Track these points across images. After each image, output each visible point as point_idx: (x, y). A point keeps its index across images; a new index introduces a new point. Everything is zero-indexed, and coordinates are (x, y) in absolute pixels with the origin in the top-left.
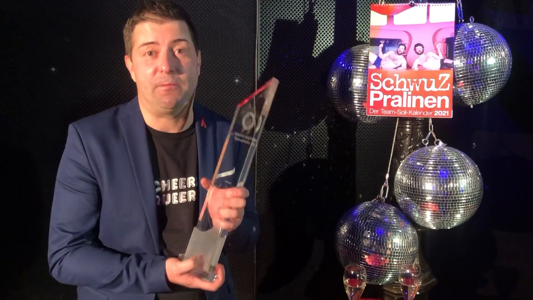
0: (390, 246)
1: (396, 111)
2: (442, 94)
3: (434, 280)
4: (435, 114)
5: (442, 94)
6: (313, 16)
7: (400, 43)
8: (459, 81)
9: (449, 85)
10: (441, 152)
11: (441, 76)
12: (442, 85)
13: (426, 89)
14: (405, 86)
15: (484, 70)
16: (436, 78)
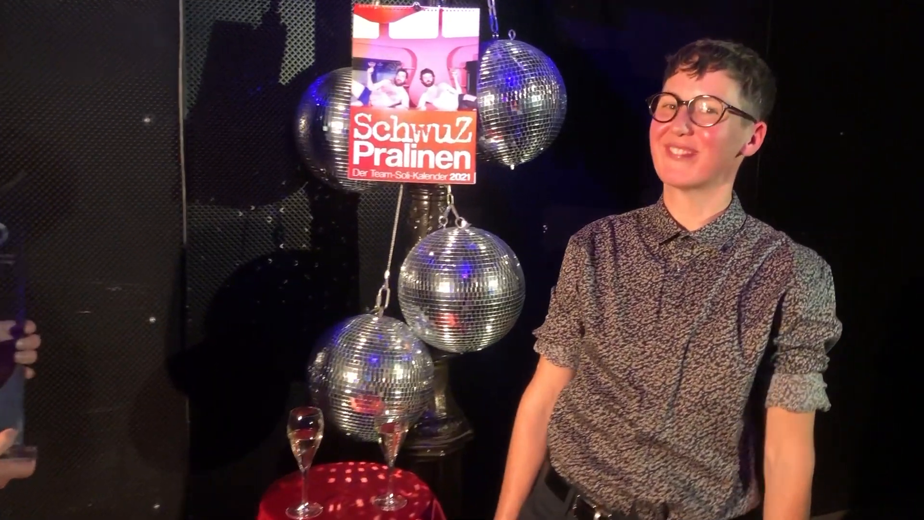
0: (384, 380)
3: (469, 432)
4: (451, 179)
6: (278, 17)
7: (399, 67)
9: (470, 134)
10: (463, 234)
11: (459, 120)
12: (460, 134)
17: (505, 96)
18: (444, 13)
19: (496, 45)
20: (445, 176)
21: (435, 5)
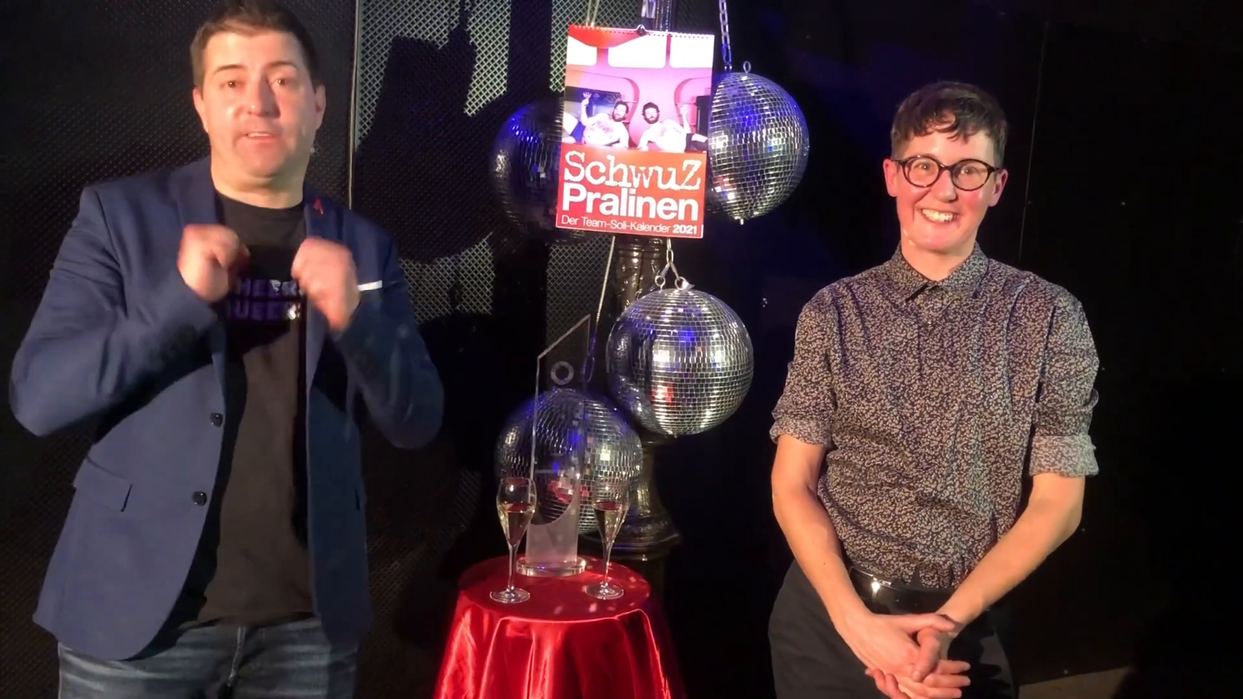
6: (467, 36)
9: (699, 180)
10: (684, 296)
11: (686, 163)
13: (660, 185)
14: (625, 177)
15: (757, 157)
16: (678, 166)
17: (741, 137)
19: (730, 79)
20: (667, 228)
21: (664, 30)
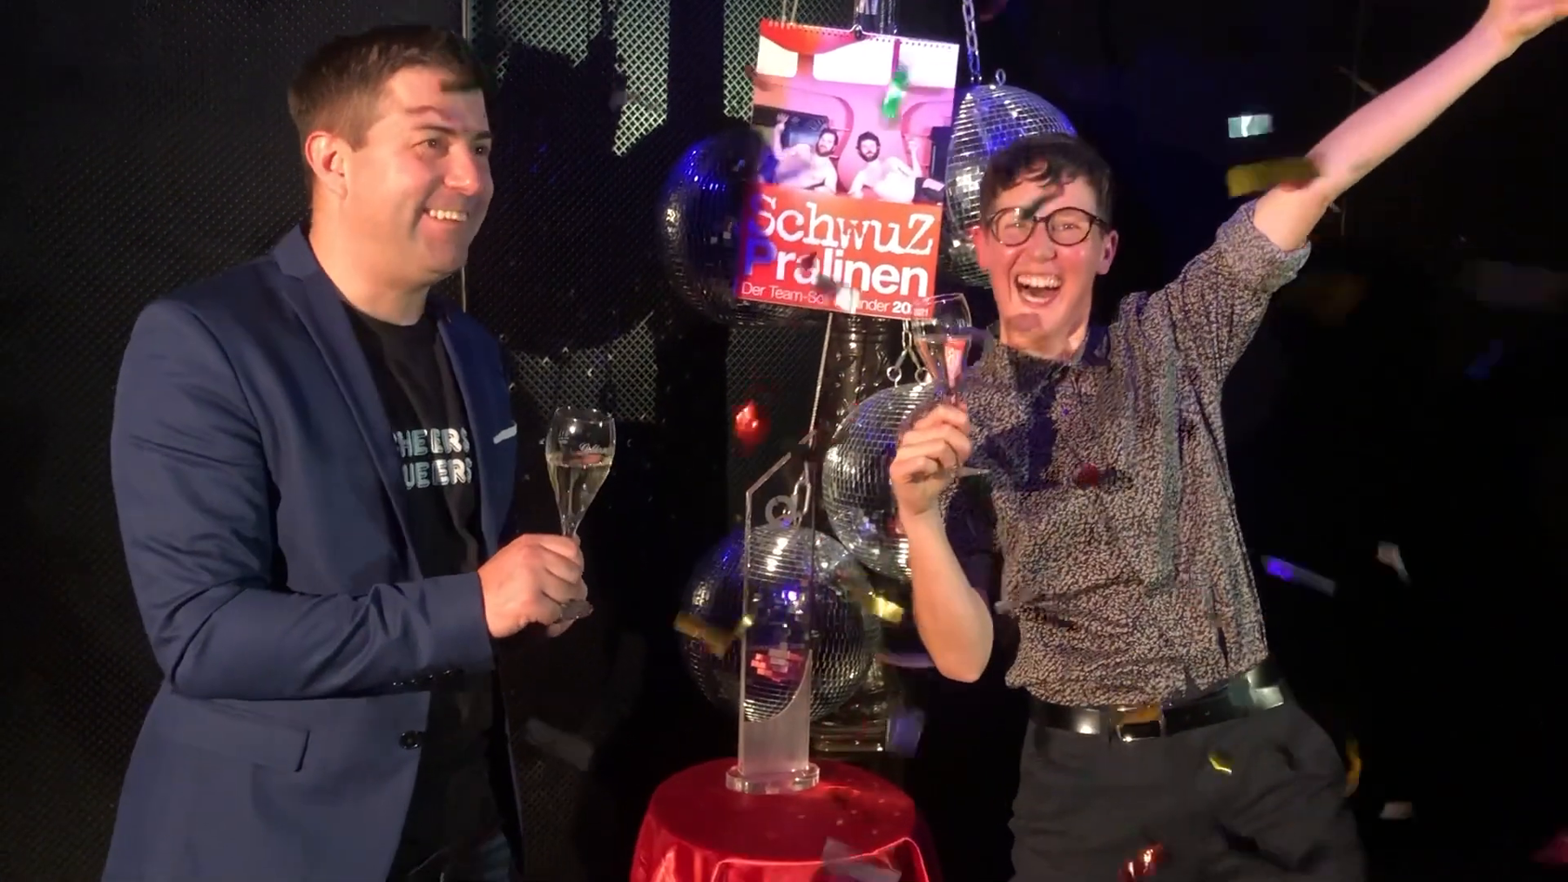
1: (805, 293)
2: (912, 261)
4: (895, 310)
5: (912, 261)
8: (970, 225)
9: (930, 242)
11: (914, 218)
12: (914, 240)
18: (902, 47)
20: (885, 306)
21: (886, 32)
